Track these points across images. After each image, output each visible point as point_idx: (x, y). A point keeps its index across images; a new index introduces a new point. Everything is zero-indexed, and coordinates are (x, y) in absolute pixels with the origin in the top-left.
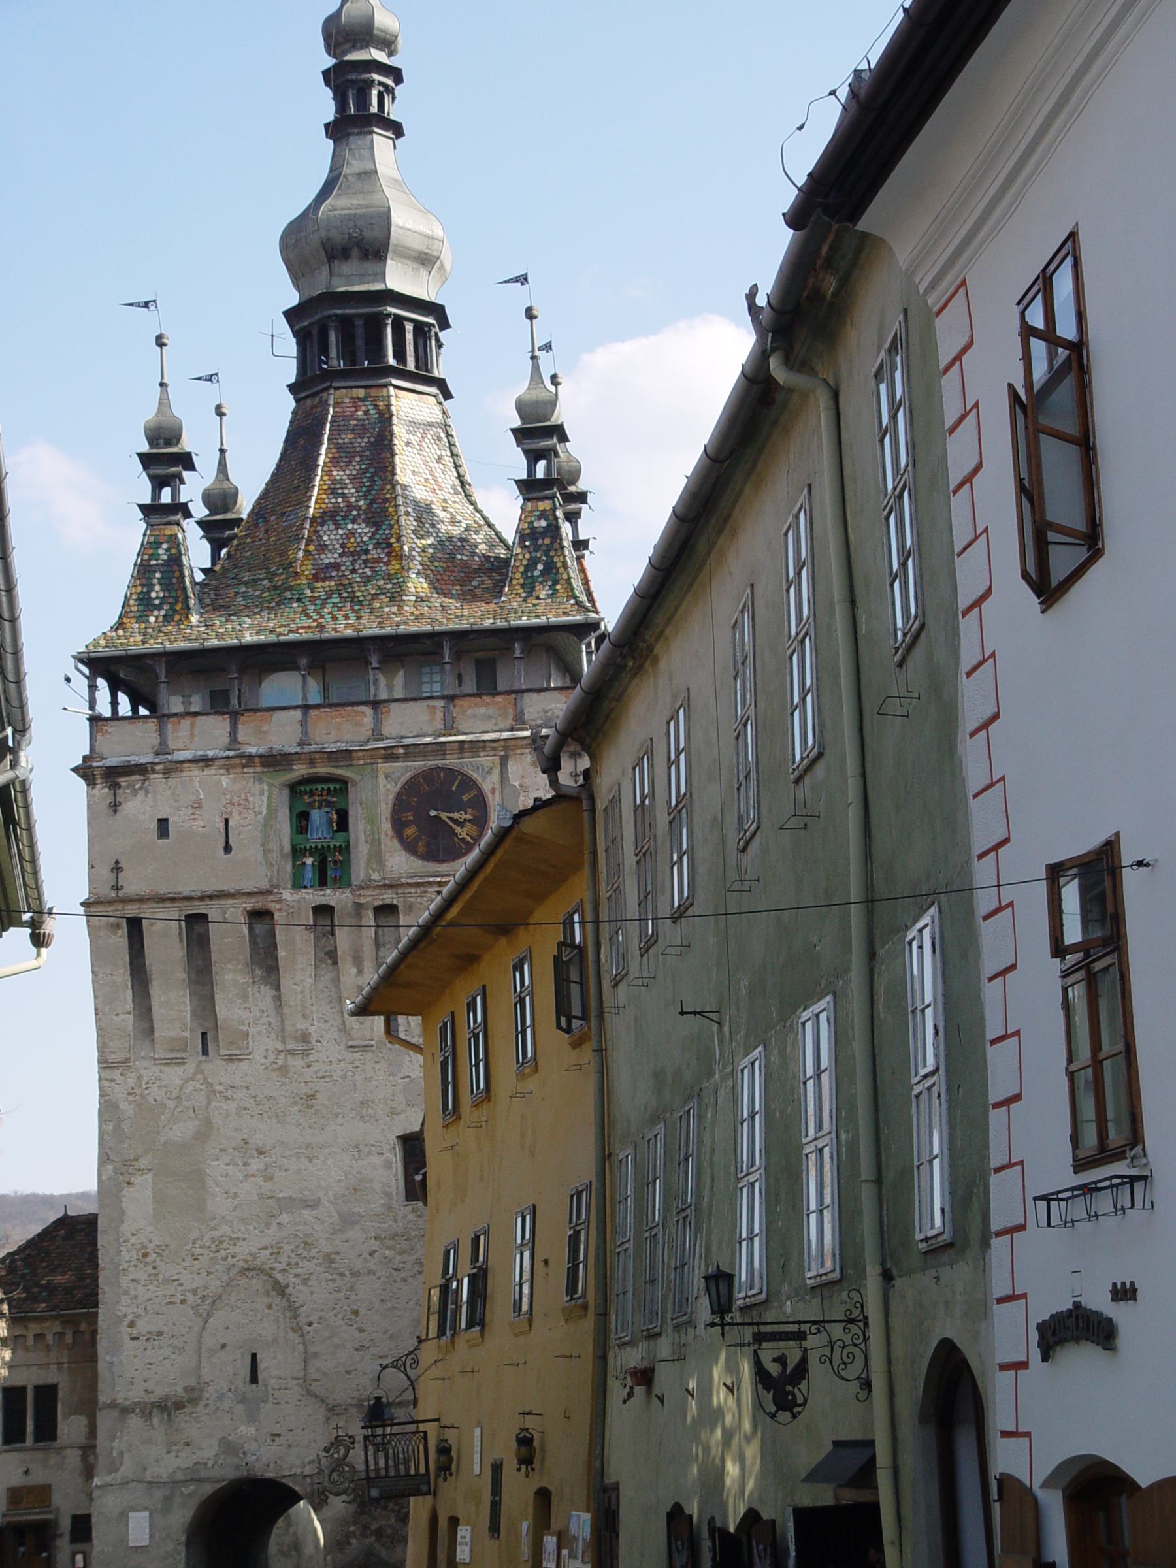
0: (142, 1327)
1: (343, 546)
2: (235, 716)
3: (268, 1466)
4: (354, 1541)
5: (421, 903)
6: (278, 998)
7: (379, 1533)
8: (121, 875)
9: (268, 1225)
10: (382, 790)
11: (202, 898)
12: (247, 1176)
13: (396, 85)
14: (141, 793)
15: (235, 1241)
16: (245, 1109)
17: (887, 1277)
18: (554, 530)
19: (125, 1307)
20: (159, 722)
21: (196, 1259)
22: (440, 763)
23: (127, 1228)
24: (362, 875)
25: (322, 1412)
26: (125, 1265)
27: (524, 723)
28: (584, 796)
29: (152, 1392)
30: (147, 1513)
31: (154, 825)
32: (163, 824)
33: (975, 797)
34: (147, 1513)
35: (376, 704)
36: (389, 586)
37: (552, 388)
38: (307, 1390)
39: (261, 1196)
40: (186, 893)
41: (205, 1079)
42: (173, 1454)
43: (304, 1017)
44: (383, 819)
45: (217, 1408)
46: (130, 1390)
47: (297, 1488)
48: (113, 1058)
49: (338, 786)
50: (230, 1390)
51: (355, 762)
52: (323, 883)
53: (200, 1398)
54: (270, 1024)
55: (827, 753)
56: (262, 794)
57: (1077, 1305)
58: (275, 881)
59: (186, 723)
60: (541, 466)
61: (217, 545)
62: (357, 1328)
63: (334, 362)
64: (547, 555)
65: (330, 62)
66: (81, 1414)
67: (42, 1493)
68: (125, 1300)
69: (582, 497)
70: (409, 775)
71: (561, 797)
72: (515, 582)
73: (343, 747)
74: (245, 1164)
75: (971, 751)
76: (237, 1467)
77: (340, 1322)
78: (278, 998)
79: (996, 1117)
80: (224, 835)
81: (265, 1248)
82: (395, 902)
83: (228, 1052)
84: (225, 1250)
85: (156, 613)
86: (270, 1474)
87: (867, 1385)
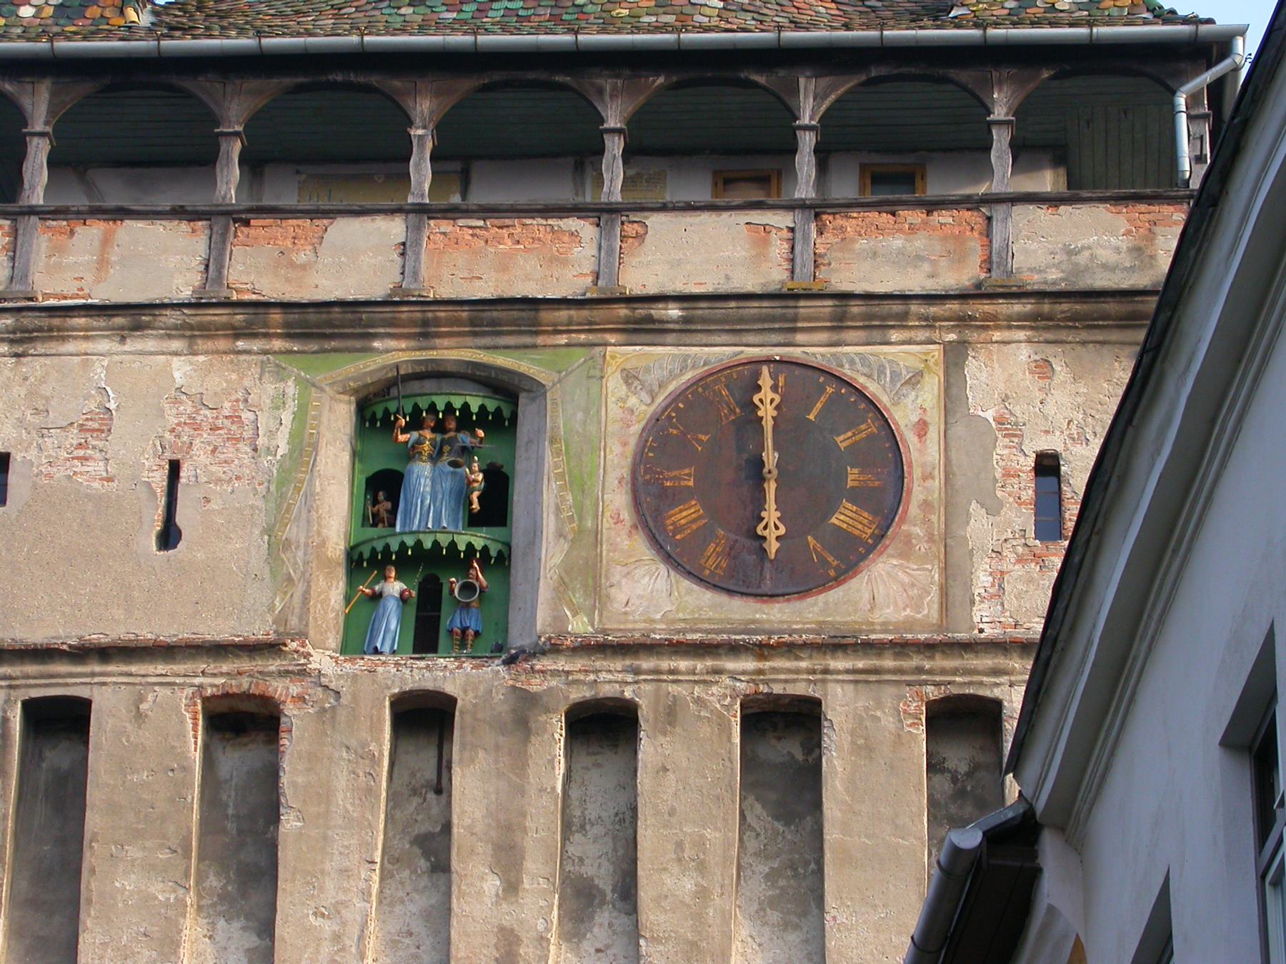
5: (699, 701)
10: (614, 410)
11: (83, 653)
20: (15, 233)
22: (776, 353)
24: (543, 619)
40: (37, 636)
44: (612, 480)
49: (491, 405)
51: (540, 340)
56: (279, 403)
58: (294, 622)
59: (92, 231)
70: (688, 376)
80: (162, 501)
82: (628, 694)
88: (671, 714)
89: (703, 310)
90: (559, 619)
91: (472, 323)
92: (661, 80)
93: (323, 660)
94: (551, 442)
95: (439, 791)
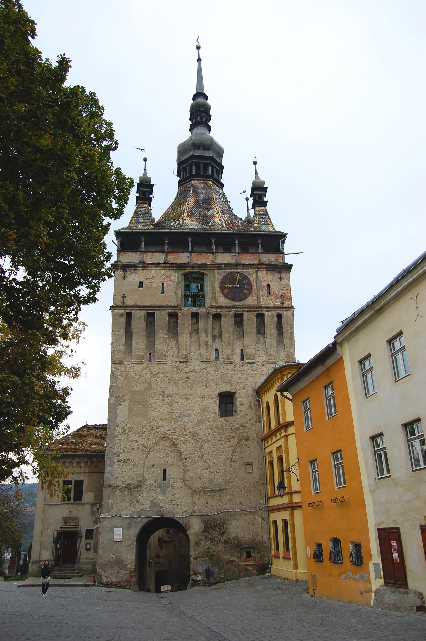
0: (122, 457)
3: (169, 512)
4: (202, 543)
5: (229, 314)
7: (212, 540)
8: (125, 299)
10: (217, 278)
11: (154, 307)
12: (163, 404)
14: (134, 274)
21: (144, 433)
22: (236, 271)
23: (118, 420)
25: (190, 491)
29: (125, 482)
31: (138, 284)
32: (141, 283)
38: (185, 484)
39: (168, 411)
40: (148, 304)
41: (150, 369)
42: (132, 506)
43: (186, 350)
45: (150, 489)
46: (117, 481)
47: (180, 521)
49: (201, 277)
50: (155, 482)
52: (194, 306)
54: (174, 352)
59: (150, 254)
62: (204, 461)
66: (91, 492)
67: (75, 519)
68: (116, 447)
70: (225, 274)
72: (255, 226)
74: (163, 400)
76: (157, 512)
77: (197, 458)
82: (221, 313)
83: (158, 361)
84: (155, 430)
85: (141, 225)
86: (171, 516)
88: (225, 315)
89: (227, 266)
90: (212, 304)
91: (198, 266)
92: (219, 237)
93: (183, 308)
94: (209, 281)
95: (197, 324)
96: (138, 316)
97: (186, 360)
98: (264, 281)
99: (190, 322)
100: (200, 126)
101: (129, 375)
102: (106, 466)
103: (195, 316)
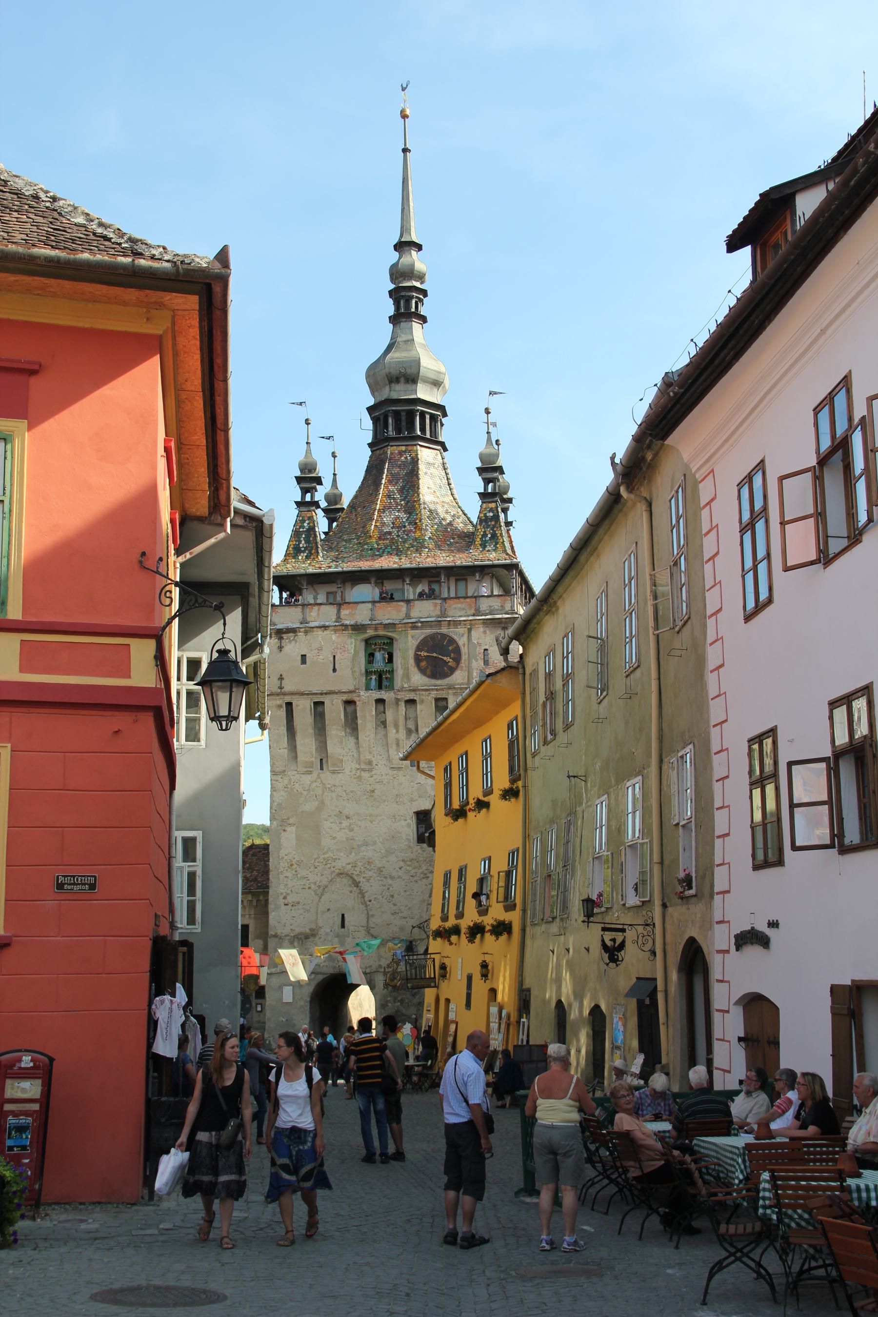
0: (290, 899)
1: (393, 523)
2: (339, 605)
6: (357, 743)
8: (283, 681)
9: (351, 853)
10: (410, 644)
11: (321, 694)
12: (341, 829)
13: (424, 297)
14: (293, 642)
15: (335, 860)
16: (341, 796)
17: (664, 906)
18: (496, 518)
19: (282, 889)
22: (438, 631)
23: (283, 853)
26: (282, 869)
27: (480, 612)
28: (520, 666)
30: (291, 987)
31: (299, 658)
33: (712, 699)
34: (291, 987)
35: (408, 601)
36: (415, 543)
37: (496, 447)
38: (369, 933)
39: (347, 838)
41: (322, 782)
43: (370, 753)
48: (278, 770)
52: (380, 687)
53: (317, 934)
55: (642, 665)
56: (352, 644)
57: (753, 928)
59: (316, 608)
60: (490, 485)
61: (331, 521)
63: (391, 433)
64: (493, 530)
65: (392, 286)
68: (282, 886)
69: (510, 500)
70: (423, 636)
71: (509, 668)
72: (476, 543)
73: (389, 621)
75: (711, 680)
76: (334, 968)
78: (357, 743)
79: (718, 842)
81: (349, 864)
85: (302, 554)
87: (654, 953)
88: (422, 701)
96: (301, 707)
97: (370, 767)
98: (479, 644)
99: (374, 713)
100: (405, 321)
101: (295, 791)
102: (270, 910)
103: (380, 701)
